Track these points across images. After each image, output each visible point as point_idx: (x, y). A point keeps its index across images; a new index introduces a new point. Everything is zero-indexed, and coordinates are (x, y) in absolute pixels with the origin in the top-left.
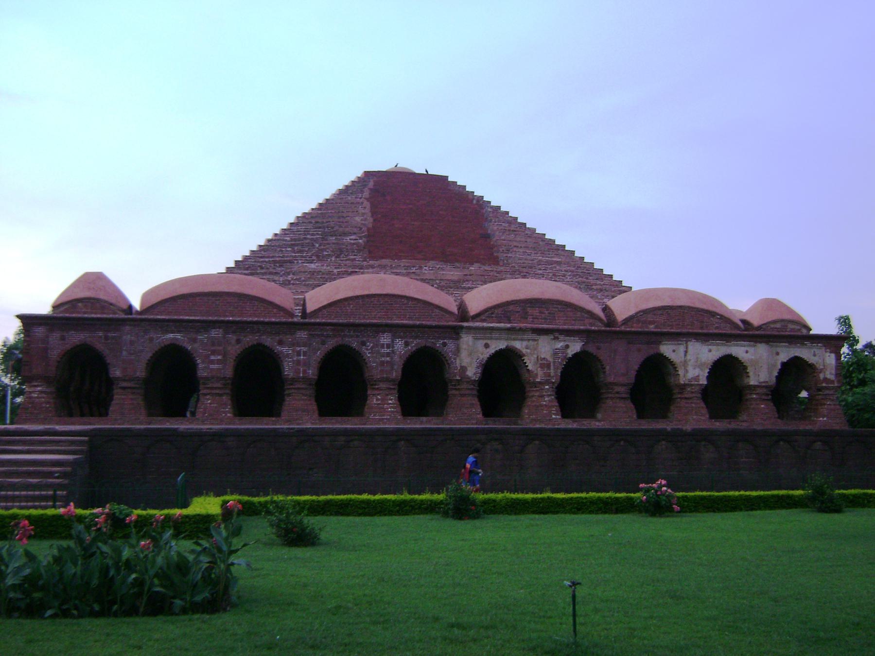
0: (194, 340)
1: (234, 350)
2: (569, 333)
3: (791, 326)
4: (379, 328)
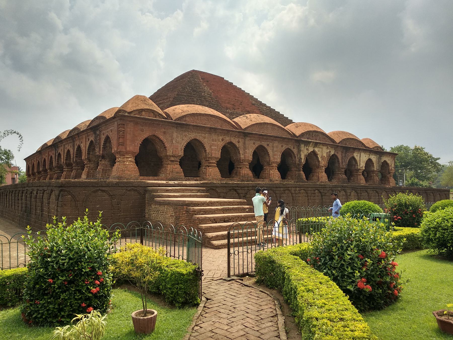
0: (205, 138)
1: (221, 144)
4: (276, 138)
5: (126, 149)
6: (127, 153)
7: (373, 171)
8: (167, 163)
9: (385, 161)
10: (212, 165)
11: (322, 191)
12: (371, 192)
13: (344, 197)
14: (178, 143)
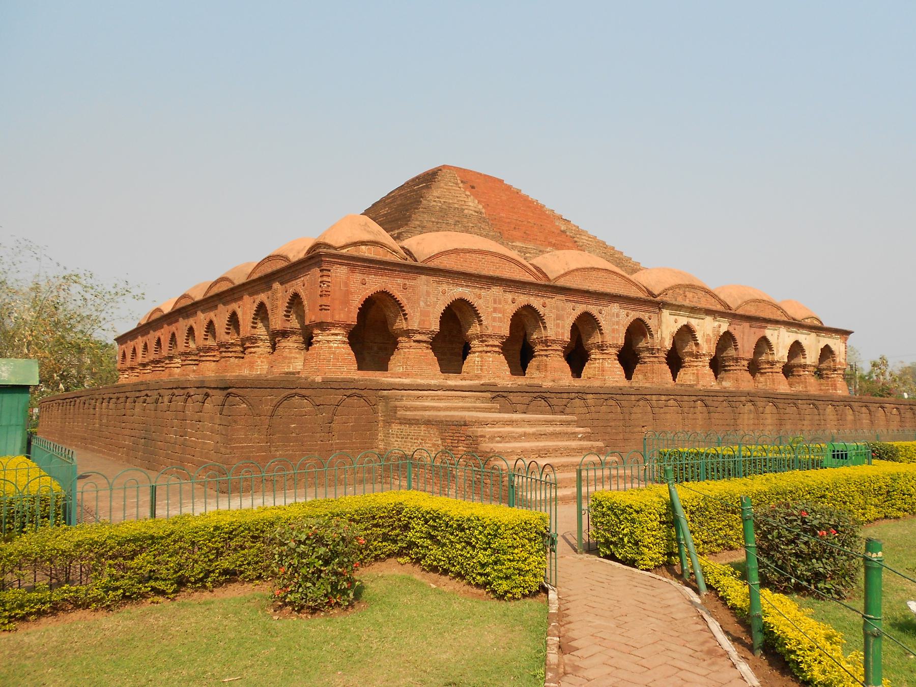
0: (480, 297)
1: (511, 309)
2: (723, 315)
3: (816, 322)
5: (333, 316)
6: (333, 325)
7: (804, 366)
8: (407, 345)
9: (827, 346)
10: (494, 349)
11: (708, 403)
12: (805, 406)
13: (752, 416)
14: (428, 306)
